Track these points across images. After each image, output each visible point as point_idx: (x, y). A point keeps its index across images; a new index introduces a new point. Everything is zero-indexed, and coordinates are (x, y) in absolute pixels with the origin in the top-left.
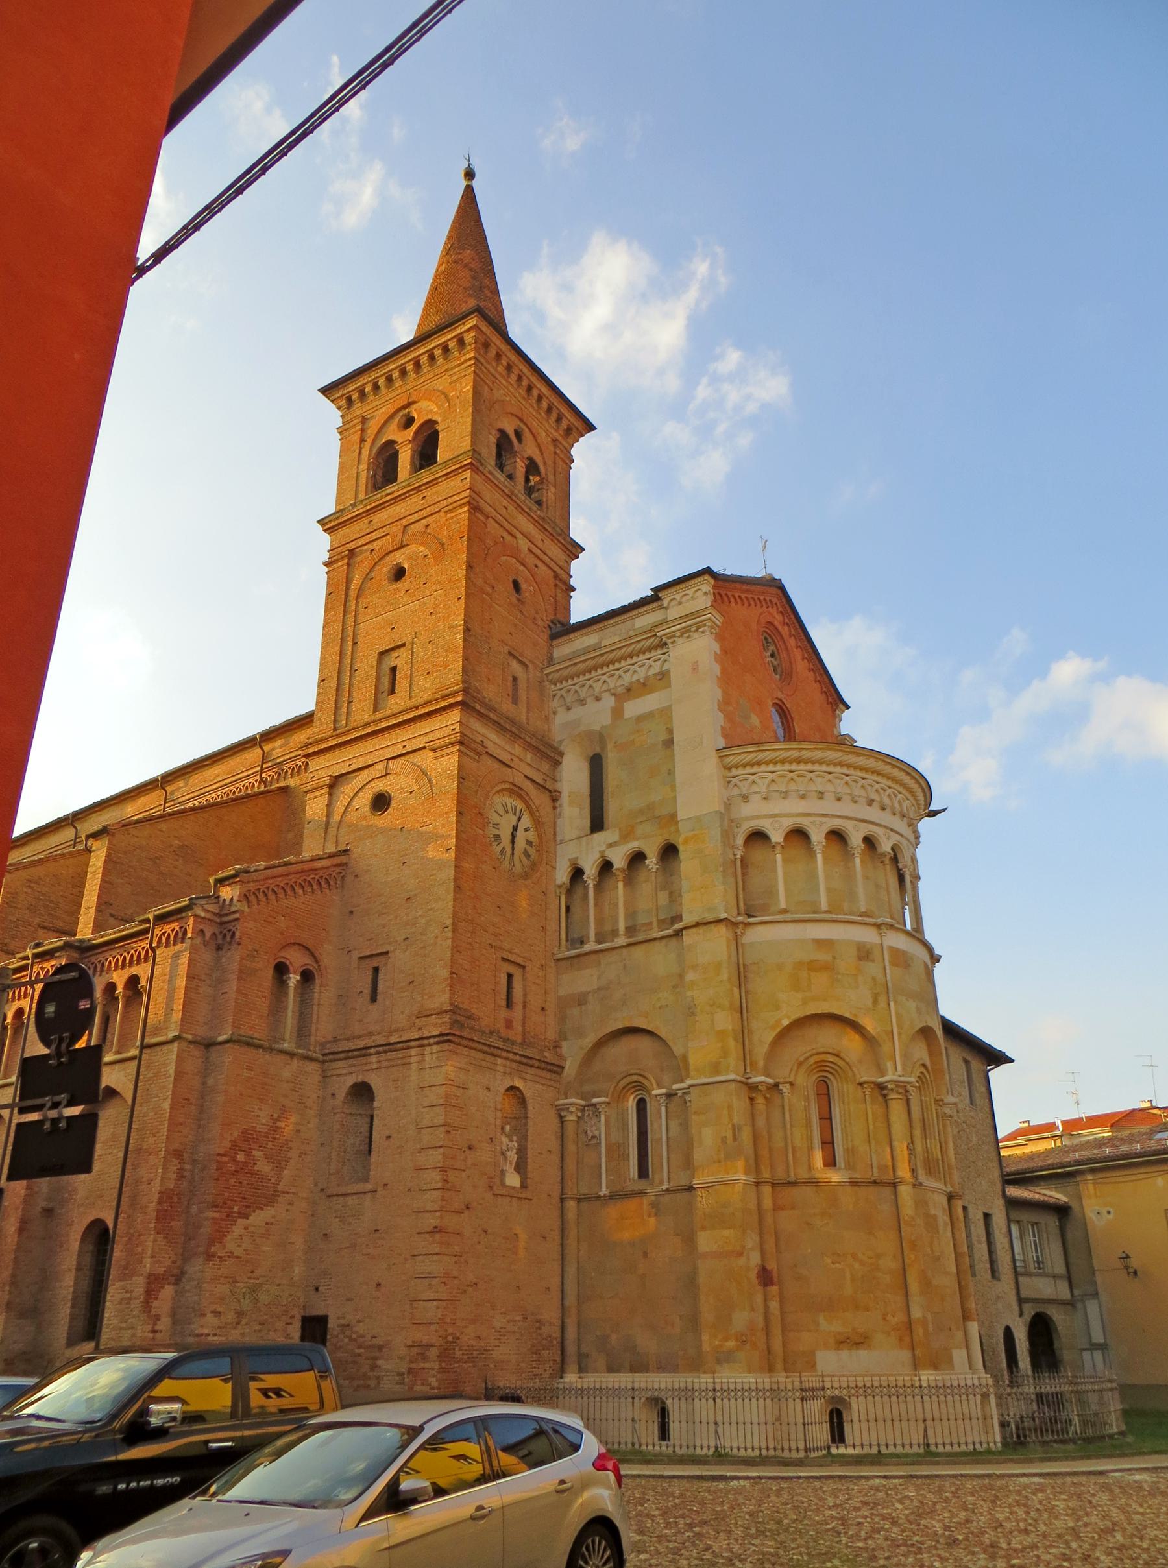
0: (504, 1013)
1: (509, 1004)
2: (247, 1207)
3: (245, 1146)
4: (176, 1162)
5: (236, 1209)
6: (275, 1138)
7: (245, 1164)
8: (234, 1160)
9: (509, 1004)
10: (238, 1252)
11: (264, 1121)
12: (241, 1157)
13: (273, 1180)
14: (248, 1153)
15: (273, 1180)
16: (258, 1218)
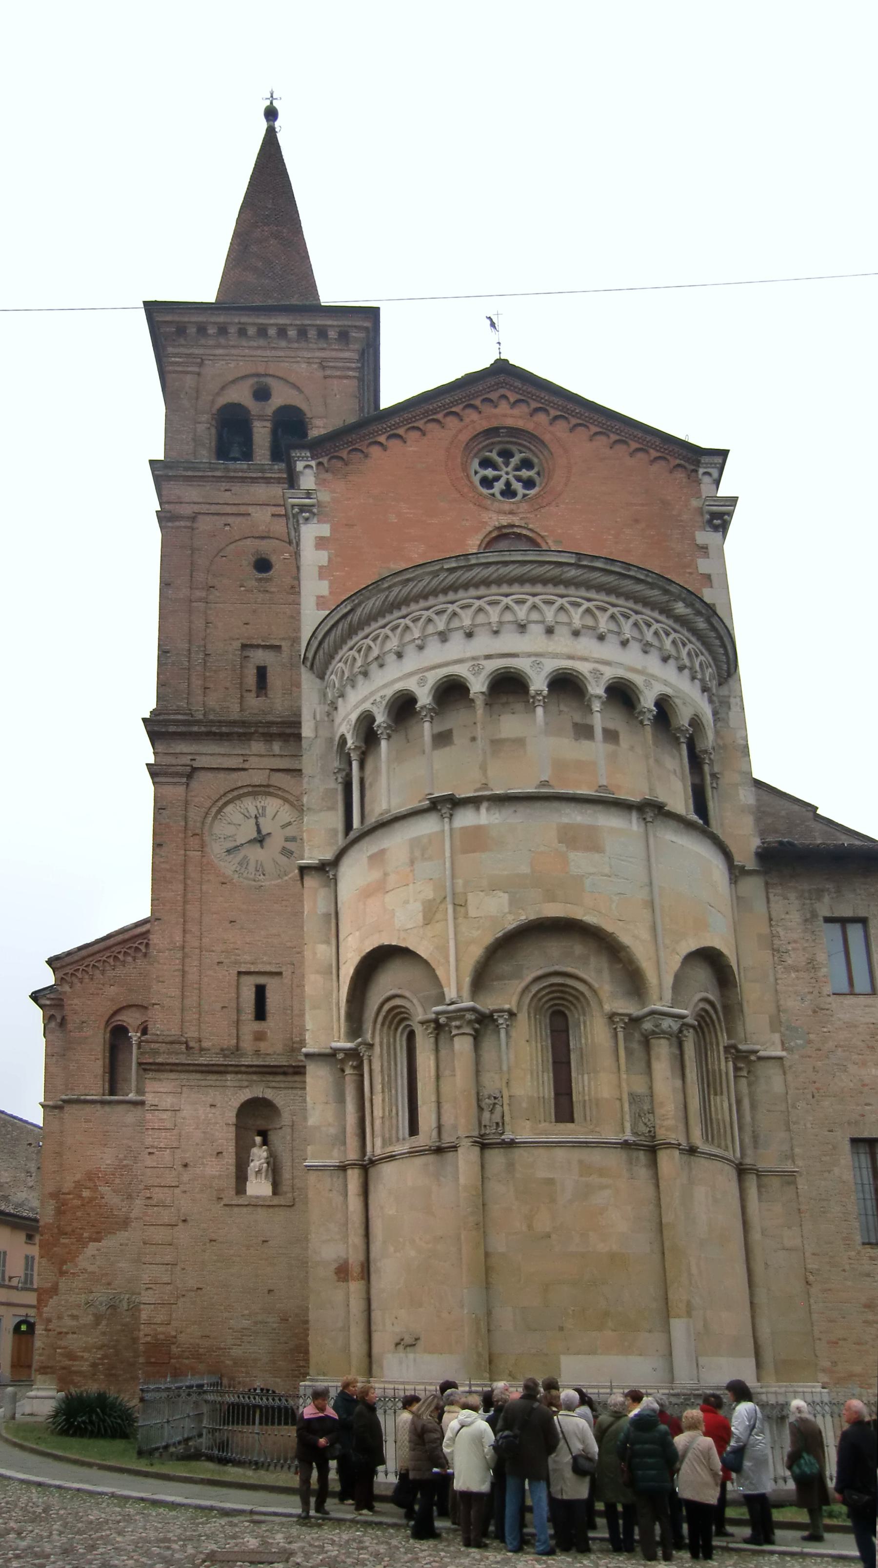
0: (250, 1026)
1: (260, 1013)
2: (98, 1233)
3: (91, 1185)
4: (53, 1202)
5: (86, 1235)
6: (122, 1175)
7: (91, 1199)
8: (80, 1197)
9: (260, 1013)
10: (91, 1268)
11: (108, 1162)
12: (86, 1193)
13: (123, 1210)
14: (95, 1189)
15: (123, 1210)
16: (109, 1243)
